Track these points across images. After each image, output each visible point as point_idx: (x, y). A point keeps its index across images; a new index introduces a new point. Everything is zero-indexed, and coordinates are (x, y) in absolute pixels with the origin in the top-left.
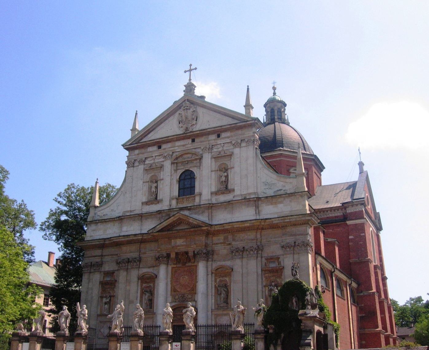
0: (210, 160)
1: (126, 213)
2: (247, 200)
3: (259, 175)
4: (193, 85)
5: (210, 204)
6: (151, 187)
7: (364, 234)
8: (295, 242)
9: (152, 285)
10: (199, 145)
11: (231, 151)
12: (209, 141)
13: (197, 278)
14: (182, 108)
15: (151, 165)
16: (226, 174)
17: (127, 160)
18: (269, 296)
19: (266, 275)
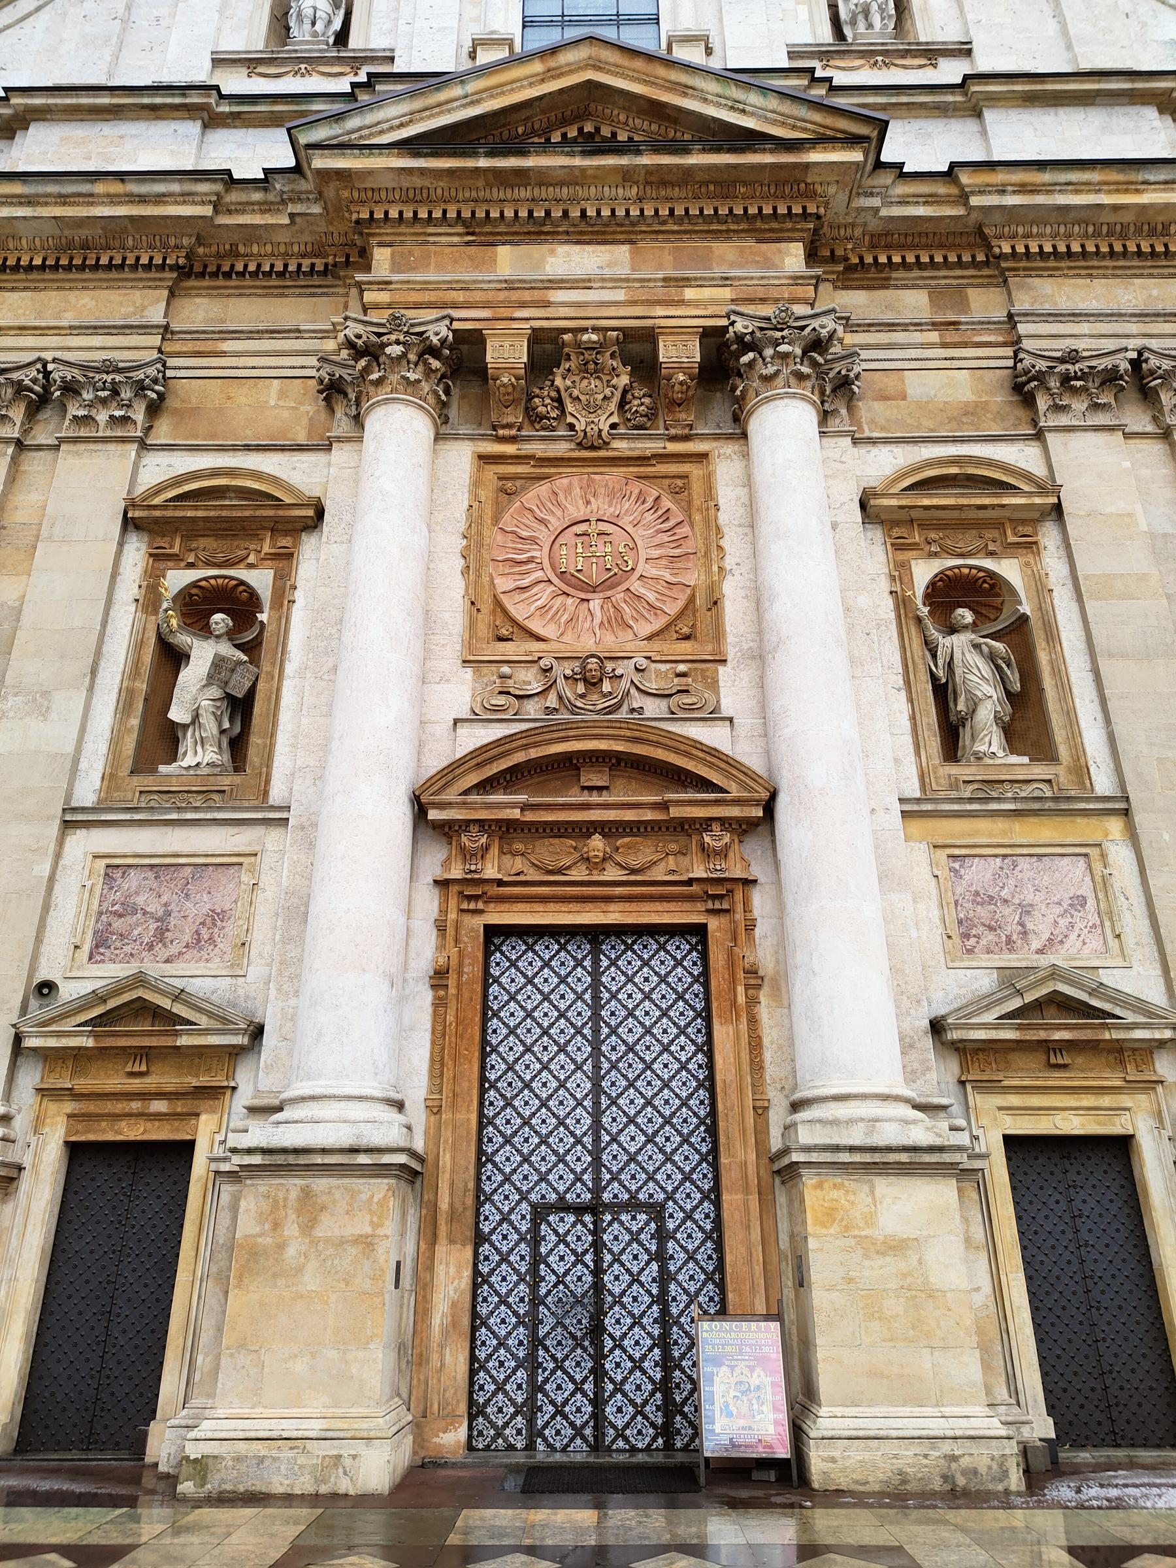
9: (261, 579)
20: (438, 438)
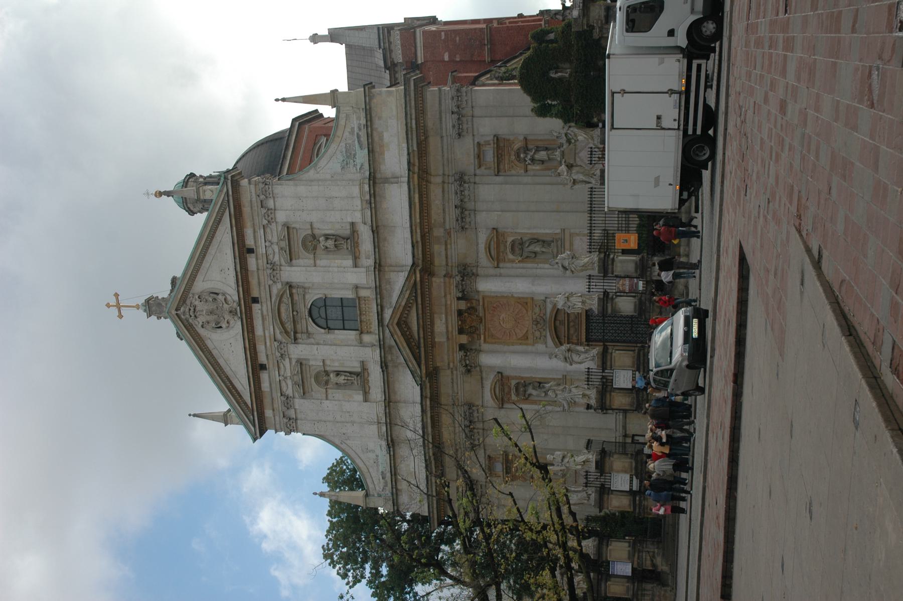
0: (293, 269)
1: (381, 432)
2: (373, 199)
3: (329, 177)
4: (148, 301)
5: (375, 268)
6: (337, 384)
7: (443, 34)
8: (453, 113)
9: (513, 383)
10: (265, 289)
11: (280, 228)
12: (258, 269)
13: (505, 295)
14: (190, 321)
15: (295, 383)
16: (322, 239)
17: (283, 433)
18: (543, 164)
19: (506, 168)
20: (480, 351)
